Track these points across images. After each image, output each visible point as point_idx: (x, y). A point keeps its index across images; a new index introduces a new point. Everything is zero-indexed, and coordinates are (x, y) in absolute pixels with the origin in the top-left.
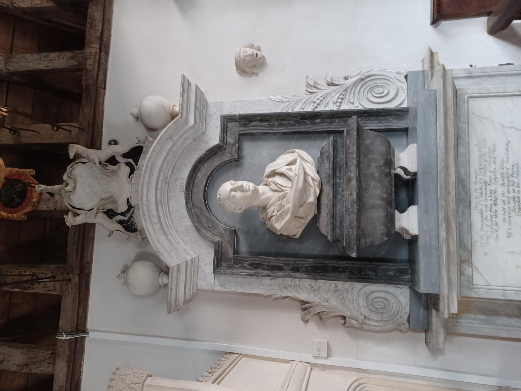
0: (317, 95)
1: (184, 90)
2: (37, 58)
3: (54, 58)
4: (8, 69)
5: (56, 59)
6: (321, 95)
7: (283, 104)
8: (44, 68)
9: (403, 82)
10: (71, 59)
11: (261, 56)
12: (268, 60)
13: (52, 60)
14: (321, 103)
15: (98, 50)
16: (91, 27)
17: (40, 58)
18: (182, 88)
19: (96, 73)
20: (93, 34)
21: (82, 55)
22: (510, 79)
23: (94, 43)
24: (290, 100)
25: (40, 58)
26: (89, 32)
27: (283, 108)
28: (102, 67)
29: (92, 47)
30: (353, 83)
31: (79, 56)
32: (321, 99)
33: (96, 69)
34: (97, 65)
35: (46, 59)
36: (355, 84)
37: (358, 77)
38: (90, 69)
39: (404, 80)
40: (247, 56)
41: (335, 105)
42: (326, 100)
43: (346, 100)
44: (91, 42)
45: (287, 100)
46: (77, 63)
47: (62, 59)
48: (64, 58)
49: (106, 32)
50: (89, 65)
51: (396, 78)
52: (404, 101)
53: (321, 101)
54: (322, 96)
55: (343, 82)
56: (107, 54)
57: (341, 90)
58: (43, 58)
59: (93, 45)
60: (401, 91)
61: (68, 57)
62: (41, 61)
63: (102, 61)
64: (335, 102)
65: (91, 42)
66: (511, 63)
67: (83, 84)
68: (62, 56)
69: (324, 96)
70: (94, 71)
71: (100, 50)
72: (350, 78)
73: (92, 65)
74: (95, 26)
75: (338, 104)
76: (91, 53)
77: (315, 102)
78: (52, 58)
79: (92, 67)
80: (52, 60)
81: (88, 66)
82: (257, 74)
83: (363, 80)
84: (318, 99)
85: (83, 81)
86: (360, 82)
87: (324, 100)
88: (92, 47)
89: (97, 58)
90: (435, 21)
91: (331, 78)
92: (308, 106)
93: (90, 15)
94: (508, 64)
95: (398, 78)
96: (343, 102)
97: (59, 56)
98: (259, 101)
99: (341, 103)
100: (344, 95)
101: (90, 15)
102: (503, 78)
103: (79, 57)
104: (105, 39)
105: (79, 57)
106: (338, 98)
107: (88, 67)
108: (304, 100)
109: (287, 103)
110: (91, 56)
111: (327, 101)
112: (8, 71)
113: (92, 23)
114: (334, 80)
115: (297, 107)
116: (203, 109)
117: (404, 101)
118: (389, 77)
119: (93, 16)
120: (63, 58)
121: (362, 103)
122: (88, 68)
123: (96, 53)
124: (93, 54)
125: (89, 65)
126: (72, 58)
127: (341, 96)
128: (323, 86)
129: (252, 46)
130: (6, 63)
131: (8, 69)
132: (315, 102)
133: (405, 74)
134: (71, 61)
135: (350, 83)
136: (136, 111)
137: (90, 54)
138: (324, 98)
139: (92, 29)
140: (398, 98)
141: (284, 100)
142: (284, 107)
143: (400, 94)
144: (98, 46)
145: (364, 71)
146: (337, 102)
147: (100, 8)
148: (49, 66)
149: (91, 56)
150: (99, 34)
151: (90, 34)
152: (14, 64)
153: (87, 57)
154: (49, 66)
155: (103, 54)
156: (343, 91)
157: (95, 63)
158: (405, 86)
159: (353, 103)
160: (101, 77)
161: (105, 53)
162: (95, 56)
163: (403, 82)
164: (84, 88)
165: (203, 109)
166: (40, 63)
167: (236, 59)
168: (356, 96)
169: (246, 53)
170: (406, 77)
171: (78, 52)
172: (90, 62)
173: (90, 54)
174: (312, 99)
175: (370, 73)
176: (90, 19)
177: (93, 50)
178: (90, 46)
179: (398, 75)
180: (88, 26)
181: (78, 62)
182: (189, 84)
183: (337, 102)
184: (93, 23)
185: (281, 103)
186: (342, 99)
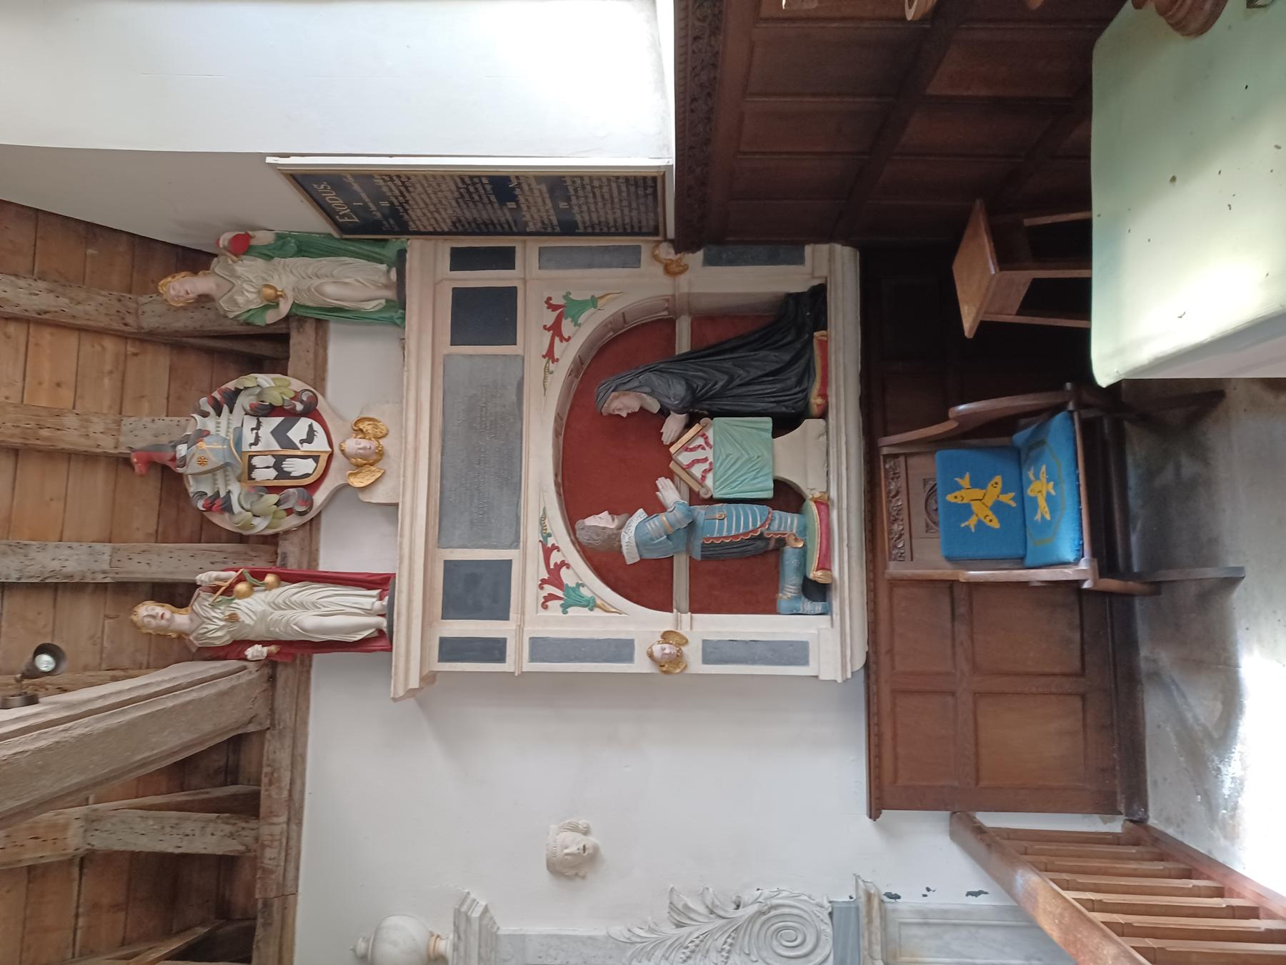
0: (690, 934)
1: (459, 938)
2: (155, 827)
3: (192, 830)
4: (89, 844)
5: (197, 833)
6: (696, 935)
7: (632, 946)
8: (170, 850)
9: (826, 924)
10: (229, 837)
11: (591, 851)
12: (603, 851)
13: (187, 835)
14: (697, 949)
15: (285, 826)
16: (271, 783)
17: (163, 828)
18: (456, 935)
19: (282, 872)
20: (275, 796)
21: (253, 833)
22: (982, 932)
23: (277, 816)
24: (643, 940)
25: (163, 828)
26: (267, 793)
27: (633, 953)
28: (293, 853)
29: (274, 824)
30: (746, 919)
31: (244, 833)
32: (697, 941)
33: (282, 864)
34: (283, 854)
35: (175, 831)
36: (752, 919)
37: (755, 908)
38: (270, 867)
39: (827, 920)
40: (567, 854)
41: (719, 955)
42: (705, 945)
43: (738, 947)
44: (272, 814)
45: (638, 940)
46: (242, 848)
47: (209, 836)
48: (215, 833)
49: (298, 782)
50: (270, 859)
51: (815, 914)
52: (828, 956)
53: (697, 946)
54: (697, 938)
55: (730, 912)
56: (300, 824)
57: (730, 928)
58: (168, 829)
59: (275, 820)
60: (823, 937)
61: (223, 834)
62: (164, 834)
63: (292, 843)
64: (719, 950)
65: (271, 812)
66: (985, 891)
67: (257, 896)
68: (209, 830)
69: (701, 937)
70: (279, 868)
71: (288, 822)
72: (743, 908)
73: (274, 858)
74: (279, 780)
75: (724, 953)
76: (272, 835)
77: (687, 947)
78: (188, 832)
79: (275, 864)
80: (187, 835)
81: (266, 861)
82: (583, 878)
83: (764, 913)
84: (692, 942)
85: (257, 891)
86: (758, 917)
87: (703, 943)
88: (274, 824)
89: (284, 841)
90: (874, 813)
91: (713, 903)
92: (674, 952)
93: (268, 759)
94: (980, 893)
95: (819, 914)
96: (733, 950)
97: (203, 828)
98: (590, 938)
99: (727, 958)
100: (733, 938)
101: (268, 759)
102: (973, 930)
103: (246, 836)
104: (296, 796)
105: (246, 836)
106: (725, 943)
107: (268, 863)
108: (669, 943)
109: (639, 945)
110: (272, 841)
111: (707, 947)
112: (89, 847)
113: (272, 774)
114: (717, 906)
115: (656, 954)
116: (491, 952)
117: (828, 956)
118: (805, 911)
119: (274, 760)
120: (213, 834)
121: (764, 954)
122: (267, 866)
123: (281, 833)
124: (277, 838)
125: (270, 859)
126: (231, 835)
127: (730, 941)
128: (699, 914)
129: (574, 829)
130: (86, 831)
131: (89, 844)
132: (687, 947)
133: (830, 910)
134: (229, 841)
135: (744, 918)
136: (361, 946)
137: (270, 838)
138: (702, 941)
139: (273, 787)
140: (818, 950)
141: (634, 939)
142: (634, 952)
143: (821, 944)
144: (283, 819)
145: (766, 892)
146: (723, 949)
147: (288, 742)
148: (180, 847)
149: (272, 841)
150: (285, 793)
151: (269, 796)
152: (105, 835)
153: (266, 843)
154: (180, 847)
155: (294, 827)
156: (732, 932)
157: (279, 853)
158: (829, 930)
159: (748, 955)
160: (290, 875)
161: (297, 824)
162: (280, 840)
163: (826, 924)
164: (260, 905)
165: (491, 952)
166: (162, 838)
167: (548, 860)
168: (753, 941)
169: (566, 848)
170: (831, 914)
171: (244, 825)
172: (269, 853)
173: (270, 838)
174: (682, 940)
175: (775, 902)
176: (268, 765)
177: (277, 830)
178: (270, 821)
179: (818, 909)
180: (265, 780)
181: (244, 845)
182: (468, 919)
183: (723, 949)
184: (275, 775)
185: (628, 945)
186: (731, 945)
